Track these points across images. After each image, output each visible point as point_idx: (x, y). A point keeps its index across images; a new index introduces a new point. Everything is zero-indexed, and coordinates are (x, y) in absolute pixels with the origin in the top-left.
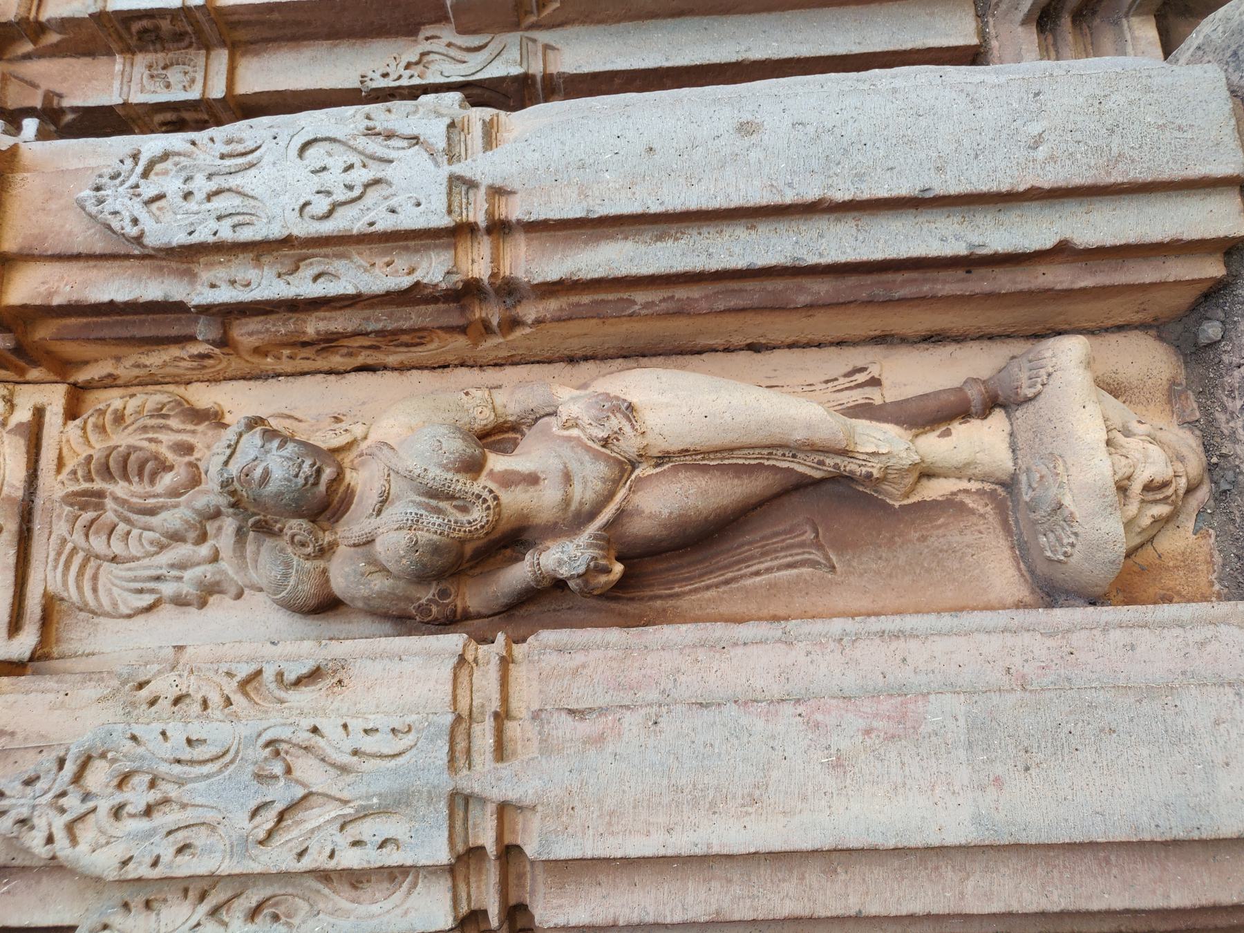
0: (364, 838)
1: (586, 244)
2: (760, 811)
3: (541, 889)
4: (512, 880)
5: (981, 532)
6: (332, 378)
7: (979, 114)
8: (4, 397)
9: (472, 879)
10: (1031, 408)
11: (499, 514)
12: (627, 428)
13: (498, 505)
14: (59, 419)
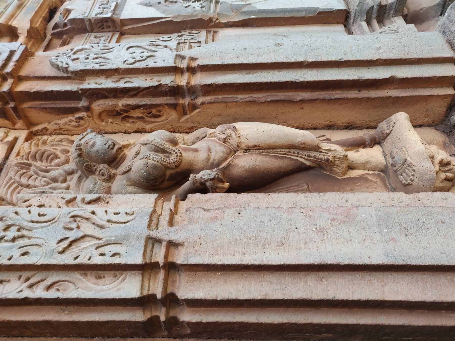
0: (105, 252)
1: (221, 74)
2: (285, 248)
3: (183, 283)
4: (170, 283)
5: (376, 188)
6: (126, 134)
7: (358, 42)
8: (5, 132)
9: (151, 281)
10: (389, 137)
11: (181, 160)
12: (233, 135)
13: (181, 156)
14: (23, 141)
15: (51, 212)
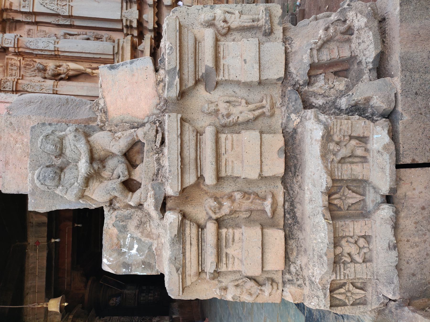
15: (37, 84)
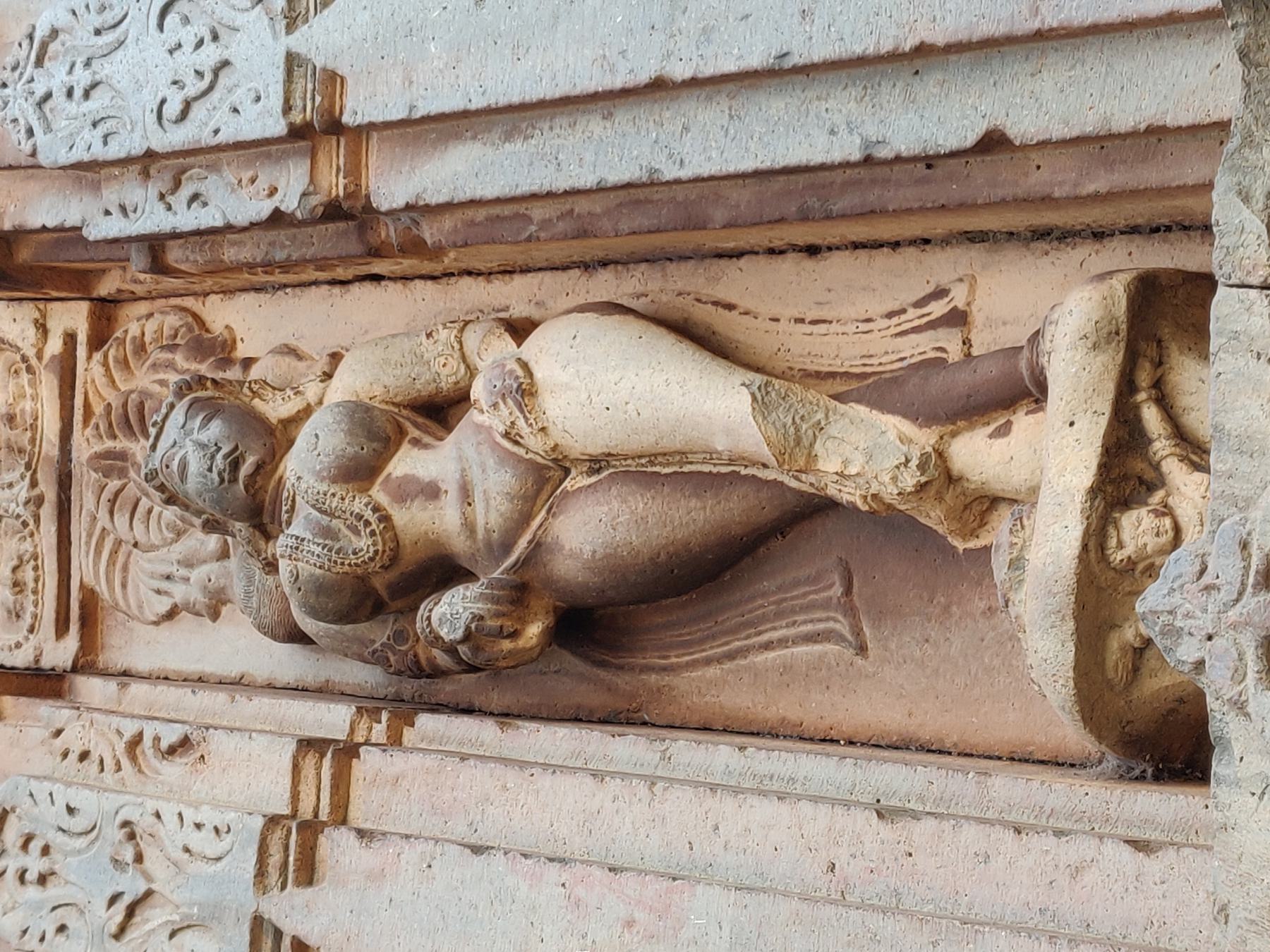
11: (396, 538)
